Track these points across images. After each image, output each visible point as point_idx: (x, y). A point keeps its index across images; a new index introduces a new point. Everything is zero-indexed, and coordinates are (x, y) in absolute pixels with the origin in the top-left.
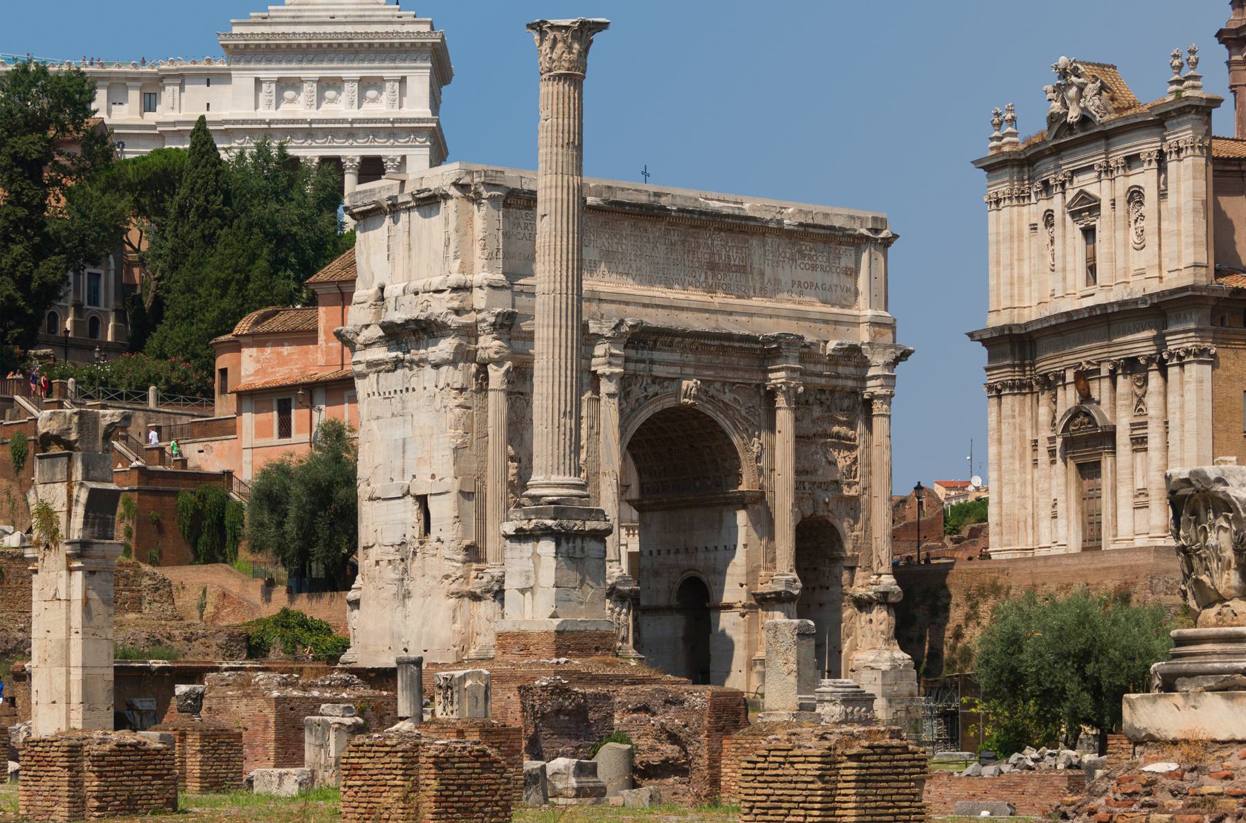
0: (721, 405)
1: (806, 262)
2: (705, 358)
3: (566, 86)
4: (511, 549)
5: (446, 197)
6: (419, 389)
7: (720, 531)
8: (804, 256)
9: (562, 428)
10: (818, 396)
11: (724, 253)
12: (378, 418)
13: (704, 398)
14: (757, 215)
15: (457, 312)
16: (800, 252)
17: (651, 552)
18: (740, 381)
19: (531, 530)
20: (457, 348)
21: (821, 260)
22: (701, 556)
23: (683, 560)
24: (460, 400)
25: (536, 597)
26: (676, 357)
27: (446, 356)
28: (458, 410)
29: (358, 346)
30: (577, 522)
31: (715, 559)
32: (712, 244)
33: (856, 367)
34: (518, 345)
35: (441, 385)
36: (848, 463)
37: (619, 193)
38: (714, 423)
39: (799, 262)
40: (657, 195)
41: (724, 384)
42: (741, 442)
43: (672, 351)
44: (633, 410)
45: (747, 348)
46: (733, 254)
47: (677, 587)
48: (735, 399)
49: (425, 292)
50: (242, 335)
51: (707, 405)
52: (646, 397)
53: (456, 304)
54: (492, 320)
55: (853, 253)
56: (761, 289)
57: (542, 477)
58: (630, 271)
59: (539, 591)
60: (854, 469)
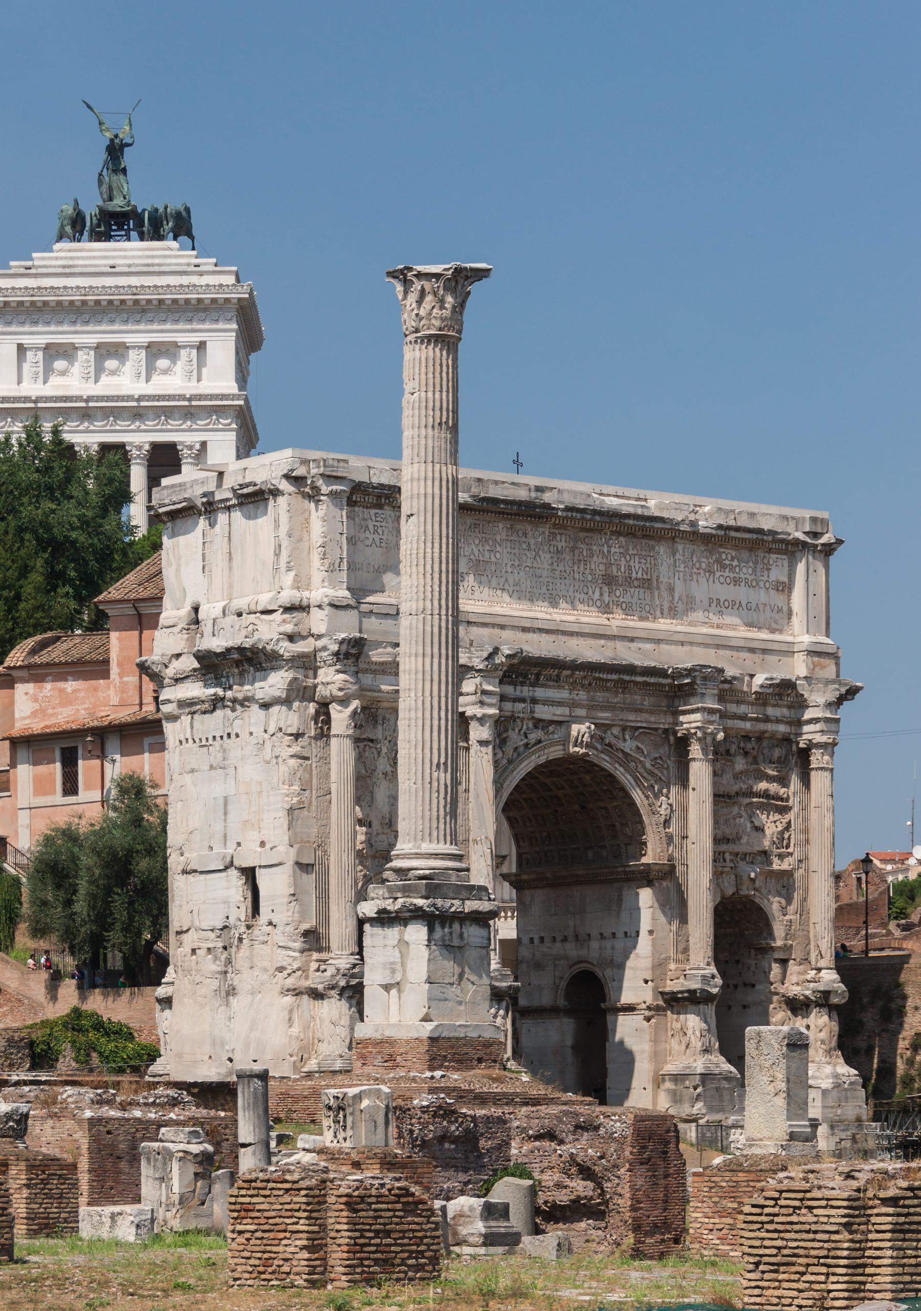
0: (620, 755)
1: (727, 574)
2: (600, 696)
3: (437, 350)
4: (372, 935)
5: (276, 493)
6: (244, 735)
7: (618, 915)
8: (723, 567)
9: (435, 784)
10: (742, 745)
11: (623, 563)
12: (193, 771)
13: (599, 747)
14: (665, 515)
15: (291, 638)
16: (719, 561)
17: (532, 940)
18: (644, 725)
19: (397, 912)
20: (291, 683)
21: (746, 572)
22: (595, 944)
23: (571, 950)
24: (296, 749)
25: (403, 995)
26: (563, 694)
27: (277, 693)
28: (293, 762)
29: (167, 681)
30: (454, 902)
31: (613, 948)
32: (609, 552)
33: (789, 707)
34: (367, 679)
35: (271, 730)
36: (780, 829)
37: (492, 487)
38: (612, 778)
39: (718, 574)
40: (539, 489)
41: (624, 729)
42: (646, 802)
43: (559, 687)
44: (510, 762)
45: (653, 684)
46: (635, 564)
47: (563, 984)
48: (638, 748)
49: (250, 613)
50: (15, 668)
51: (603, 756)
52: (526, 745)
53: (289, 628)
54: (335, 647)
55: (786, 563)
56: (670, 609)
57: (410, 845)
58: (506, 586)
59: (407, 987)
60: (786, 836)
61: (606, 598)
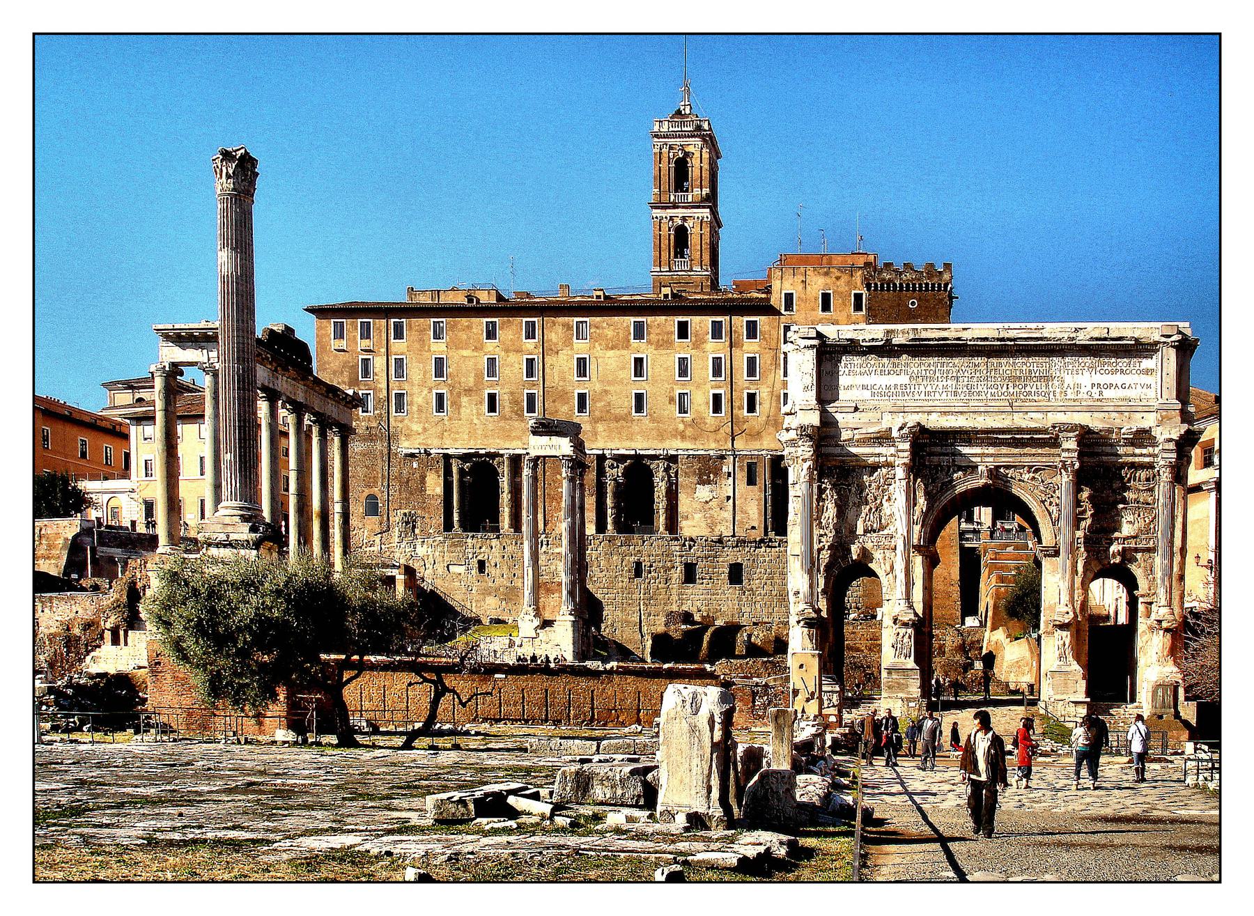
1: (1106, 367)
36: (1147, 521)
39: (1098, 369)
61: (1011, 390)
